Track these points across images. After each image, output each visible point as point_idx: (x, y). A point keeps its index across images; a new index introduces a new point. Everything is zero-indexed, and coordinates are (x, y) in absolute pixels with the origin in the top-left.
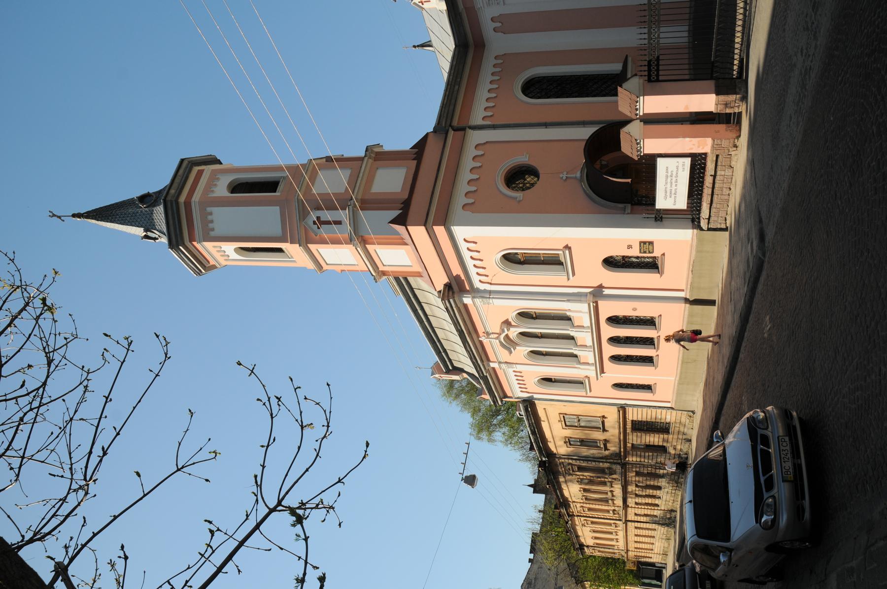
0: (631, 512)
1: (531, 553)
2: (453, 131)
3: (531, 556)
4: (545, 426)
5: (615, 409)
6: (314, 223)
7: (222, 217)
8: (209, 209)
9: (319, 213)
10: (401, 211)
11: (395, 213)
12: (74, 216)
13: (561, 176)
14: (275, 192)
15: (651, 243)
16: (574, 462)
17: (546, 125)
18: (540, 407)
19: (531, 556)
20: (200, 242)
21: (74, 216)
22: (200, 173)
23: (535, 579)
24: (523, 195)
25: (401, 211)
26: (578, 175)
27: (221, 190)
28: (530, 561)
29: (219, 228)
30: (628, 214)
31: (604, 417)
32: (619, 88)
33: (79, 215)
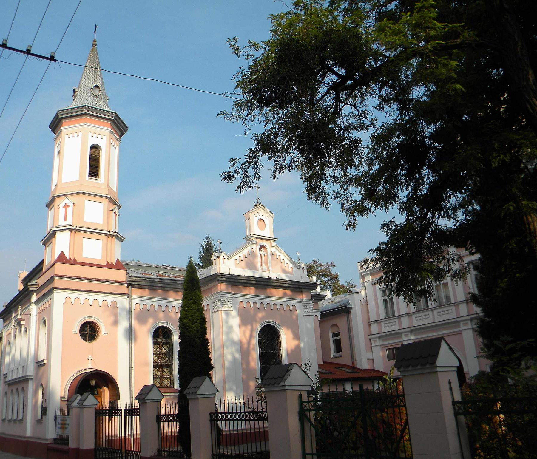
9: (71, 205)
13: (90, 356)
25: (68, 259)
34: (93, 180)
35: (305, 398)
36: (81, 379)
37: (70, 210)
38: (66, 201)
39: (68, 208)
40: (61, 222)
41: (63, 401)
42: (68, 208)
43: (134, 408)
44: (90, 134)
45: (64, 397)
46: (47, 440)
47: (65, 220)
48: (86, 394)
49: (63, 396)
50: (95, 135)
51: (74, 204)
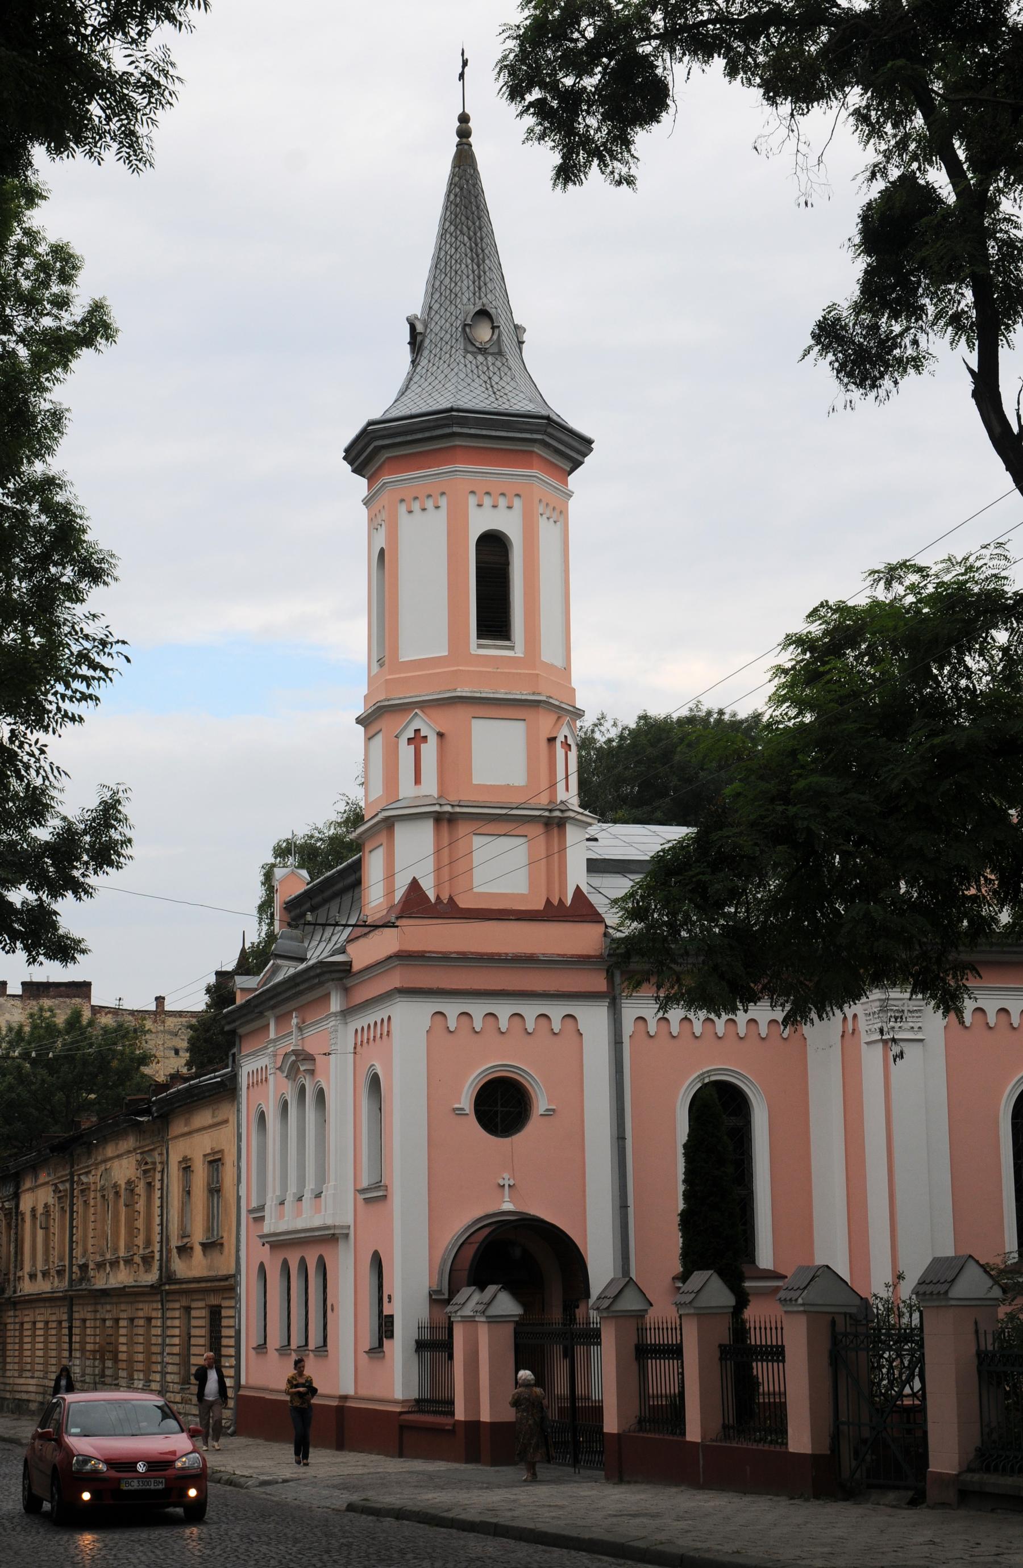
1: (24, 984)
2: (606, 968)
4: (203, 1118)
5: (232, 1272)
6: (417, 731)
9: (433, 739)
10: (433, 899)
12: (464, 119)
14: (479, 637)
15: (391, 1336)
16: (158, 1176)
17: (620, 1138)
18: (225, 1111)
19: (14, 988)
21: (464, 119)
24: (467, 1114)
25: (433, 899)
26: (507, 1206)
27: (481, 523)
30: (430, 1295)
31: (222, 1245)
32: (500, 1286)
33: (464, 134)
34: (493, 650)
35: (840, 1327)
36: (484, 1240)
37: (430, 750)
38: (417, 724)
39: (423, 746)
40: (407, 789)
41: (435, 1300)
42: (423, 746)
43: (592, 1326)
44: (472, 500)
45: (439, 1292)
46: (396, 1402)
47: (418, 780)
48: (492, 1289)
49: (435, 1288)
50: (487, 501)
51: (441, 735)
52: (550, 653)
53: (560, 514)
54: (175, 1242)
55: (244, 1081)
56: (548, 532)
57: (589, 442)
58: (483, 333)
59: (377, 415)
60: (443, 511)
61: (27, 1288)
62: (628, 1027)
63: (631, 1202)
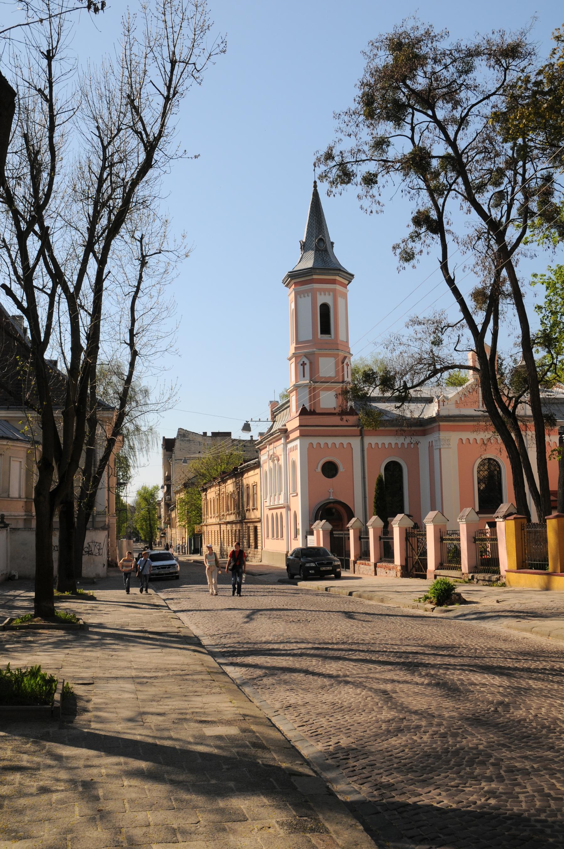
0: (223, 527)
3: (209, 434)
5: (259, 516)
7: (307, 301)
8: (310, 294)
11: (307, 406)
17: (364, 478)
18: (257, 471)
19: (209, 434)
20: (294, 289)
22: (334, 282)
23: (189, 440)
26: (331, 498)
27: (322, 299)
28: (205, 434)
29: (302, 301)
33: (315, 186)
34: (326, 337)
48: (324, 521)
52: (342, 337)
53: (345, 296)
54: (245, 509)
55: (262, 463)
56: (340, 301)
57: (353, 275)
58: (322, 244)
59: (291, 270)
60: (310, 298)
61: (210, 521)
62: (366, 446)
63: (367, 496)
